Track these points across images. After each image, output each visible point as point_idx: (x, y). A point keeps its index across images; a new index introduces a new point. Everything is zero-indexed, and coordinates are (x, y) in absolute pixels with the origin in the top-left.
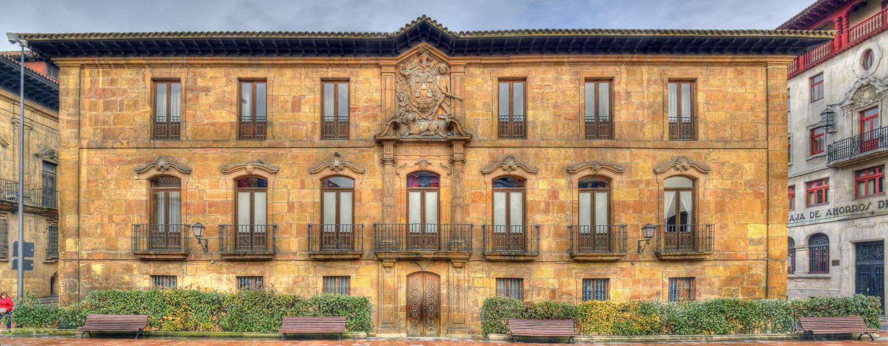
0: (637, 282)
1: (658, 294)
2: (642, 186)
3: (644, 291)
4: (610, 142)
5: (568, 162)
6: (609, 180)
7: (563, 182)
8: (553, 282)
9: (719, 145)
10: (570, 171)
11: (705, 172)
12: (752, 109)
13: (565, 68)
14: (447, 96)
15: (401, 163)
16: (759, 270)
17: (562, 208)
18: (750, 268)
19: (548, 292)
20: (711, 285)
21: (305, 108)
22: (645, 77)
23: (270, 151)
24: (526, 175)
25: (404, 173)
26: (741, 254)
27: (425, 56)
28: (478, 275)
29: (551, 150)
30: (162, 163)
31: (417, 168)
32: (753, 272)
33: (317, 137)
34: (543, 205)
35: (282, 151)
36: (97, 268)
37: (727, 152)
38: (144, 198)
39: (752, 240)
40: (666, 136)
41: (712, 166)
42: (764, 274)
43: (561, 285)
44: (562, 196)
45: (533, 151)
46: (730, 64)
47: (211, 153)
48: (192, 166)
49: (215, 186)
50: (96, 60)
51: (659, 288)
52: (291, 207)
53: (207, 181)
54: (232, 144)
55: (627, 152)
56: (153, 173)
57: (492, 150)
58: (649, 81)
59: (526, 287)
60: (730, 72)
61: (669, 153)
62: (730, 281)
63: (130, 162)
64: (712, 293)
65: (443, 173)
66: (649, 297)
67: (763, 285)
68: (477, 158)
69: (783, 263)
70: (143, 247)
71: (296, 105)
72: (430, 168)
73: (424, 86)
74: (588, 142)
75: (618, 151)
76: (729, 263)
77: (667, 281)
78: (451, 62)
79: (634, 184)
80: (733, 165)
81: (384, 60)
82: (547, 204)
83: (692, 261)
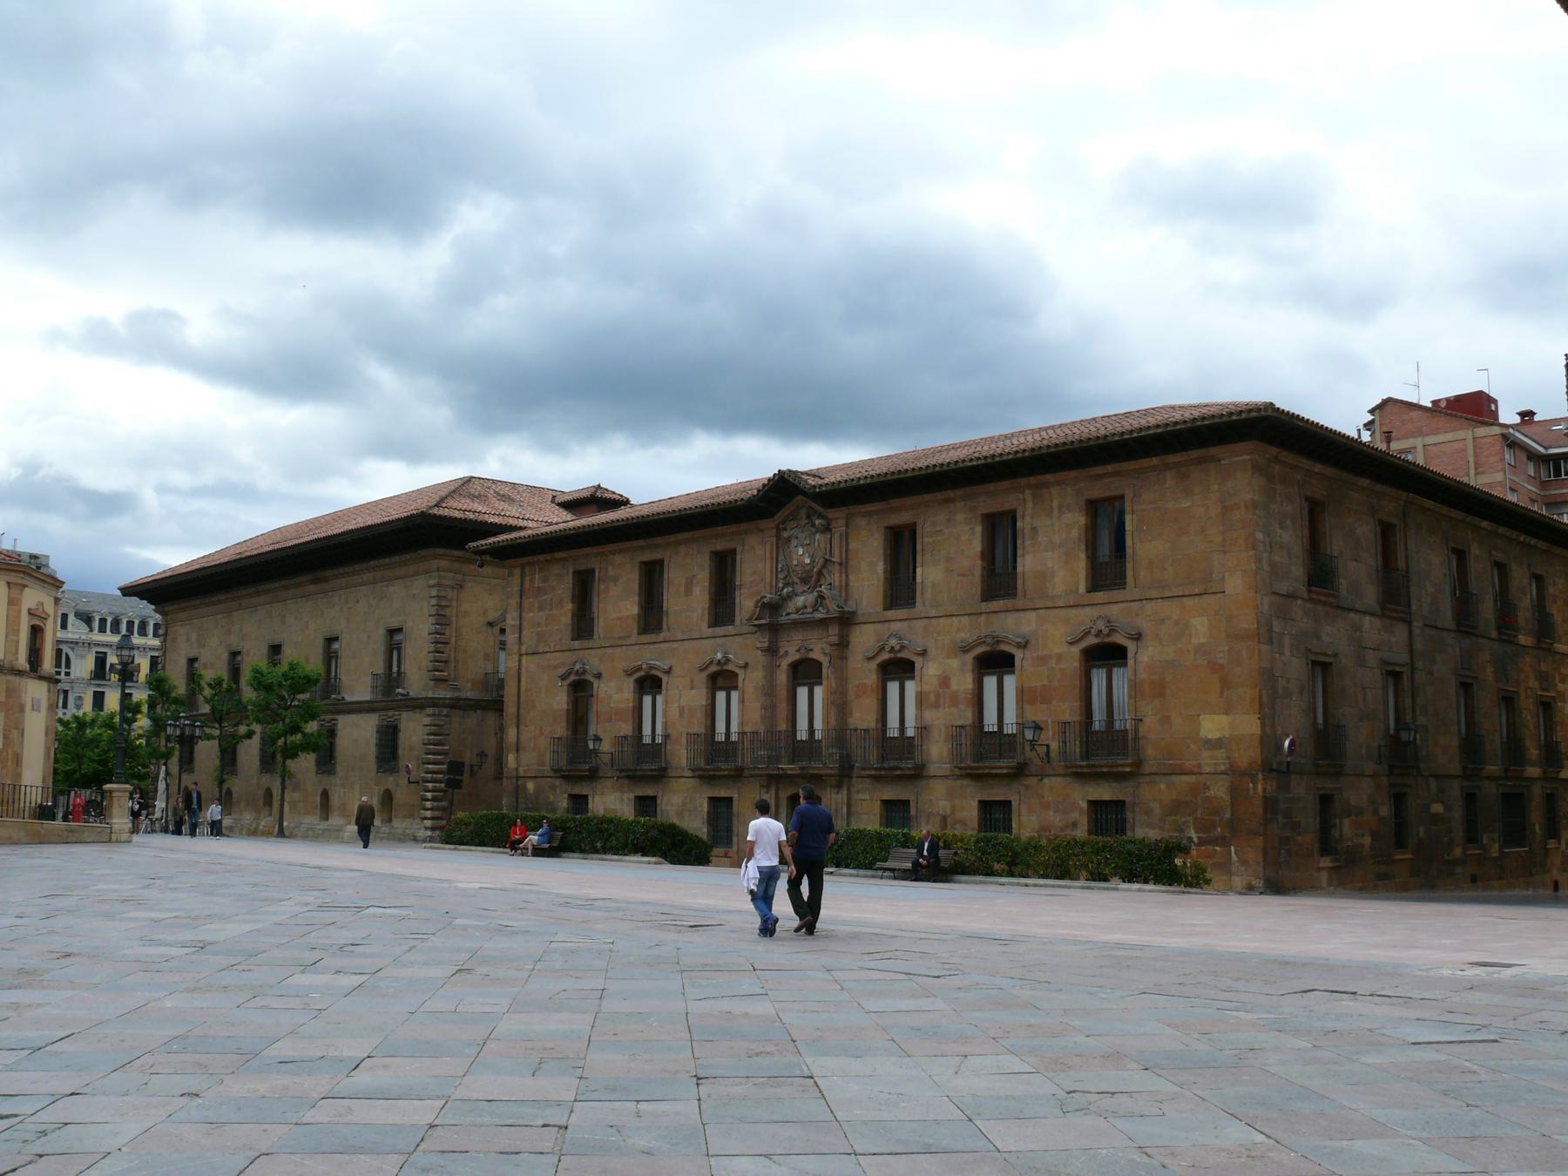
0: (1046, 806)
1: (1074, 825)
2: (1052, 663)
3: (1056, 819)
4: (1009, 603)
5: (962, 635)
6: (1012, 657)
7: (955, 663)
8: (943, 806)
9: (1155, 594)
10: (965, 650)
11: (1138, 637)
12: (1203, 530)
13: (959, 504)
14: (826, 561)
15: (782, 651)
16: (1219, 790)
17: (954, 700)
18: (1206, 787)
19: (938, 819)
20: (1148, 812)
21: (697, 591)
22: (1055, 503)
23: (666, 645)
24: (914, 658)
25: (785, 663)
26: (1190, 764)
27: (803, 512)
28: (861, 796)
29: (942, 621)
30: (577, 667)
31: (797, 657)
32: (1211, 793)
33: (705, 624)
34: (932, 697)
35: (675, 645)
36: (531, 786)
37: (1168, 603)
38: (565, 707)
39: (1207, 741)
40: (1082, 589)
41: (1145, 625)
42: (1227, 798)
43: (953, 809)
44: (954, 686)
45: (921, 623)
46: (1167, 467)
47: (618, 652)
48: (603, 669)
49: (620, 690)
50: (530, 559)
51: (1075, 816)
52: (682, 710)
53: (613, 684)
54: (632, 640)
55: (1033, 615)
56: (573, 678)
57: (879, 626)
58: (1060, 507)
59: (913, 812)
60: (1170, 479)
61: (1088, 611)
62: (1175, 807)
63: (556, 667)
64: (1151, 826)
65: (825, 661)
66: (1062, 830)
67: (1228, 815)
68: (864, 639)
69: (1254, 778)
70: (563, 764)
71: (688, 591)
72: (812, 655)
73: (801, 551)
74: (984, 607)
75: (1022, 614)
76: (1175, 779)
77: (1084, 805)
78: (830, 516)
79: (1042, 660)
80: (1177, 623)
81: (763, 524)
82: (938, 696)
83: (1120, 777)
